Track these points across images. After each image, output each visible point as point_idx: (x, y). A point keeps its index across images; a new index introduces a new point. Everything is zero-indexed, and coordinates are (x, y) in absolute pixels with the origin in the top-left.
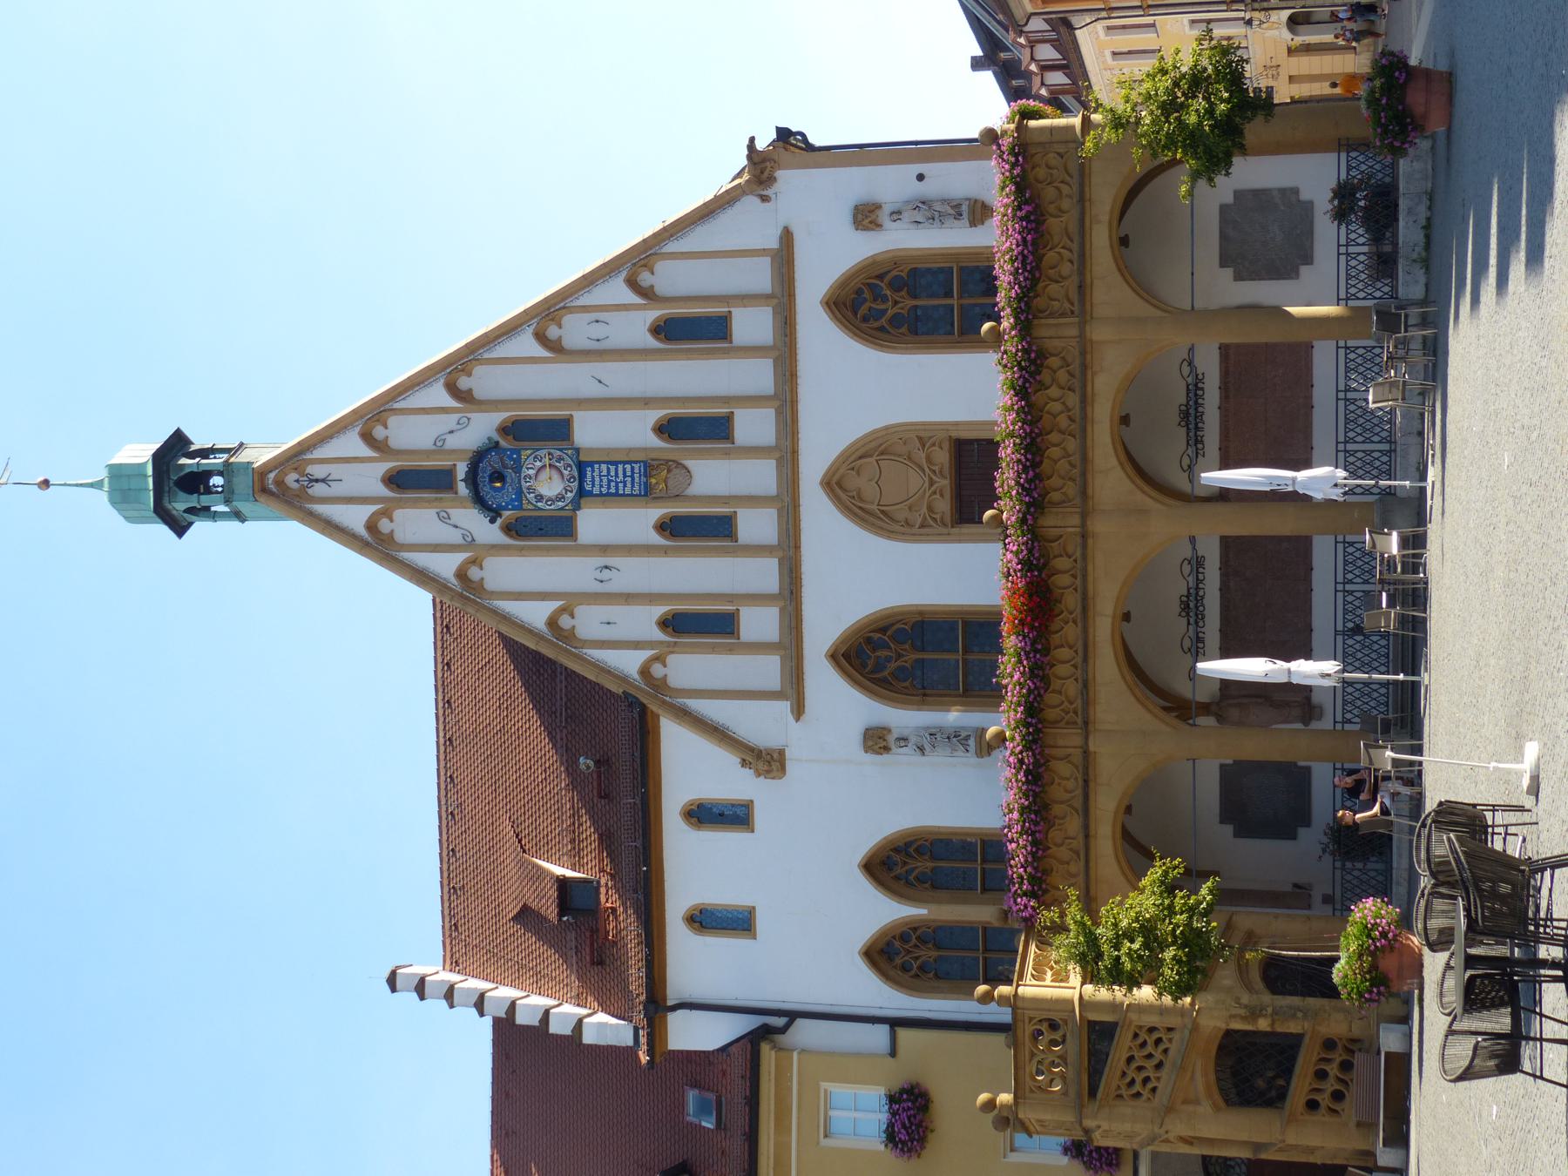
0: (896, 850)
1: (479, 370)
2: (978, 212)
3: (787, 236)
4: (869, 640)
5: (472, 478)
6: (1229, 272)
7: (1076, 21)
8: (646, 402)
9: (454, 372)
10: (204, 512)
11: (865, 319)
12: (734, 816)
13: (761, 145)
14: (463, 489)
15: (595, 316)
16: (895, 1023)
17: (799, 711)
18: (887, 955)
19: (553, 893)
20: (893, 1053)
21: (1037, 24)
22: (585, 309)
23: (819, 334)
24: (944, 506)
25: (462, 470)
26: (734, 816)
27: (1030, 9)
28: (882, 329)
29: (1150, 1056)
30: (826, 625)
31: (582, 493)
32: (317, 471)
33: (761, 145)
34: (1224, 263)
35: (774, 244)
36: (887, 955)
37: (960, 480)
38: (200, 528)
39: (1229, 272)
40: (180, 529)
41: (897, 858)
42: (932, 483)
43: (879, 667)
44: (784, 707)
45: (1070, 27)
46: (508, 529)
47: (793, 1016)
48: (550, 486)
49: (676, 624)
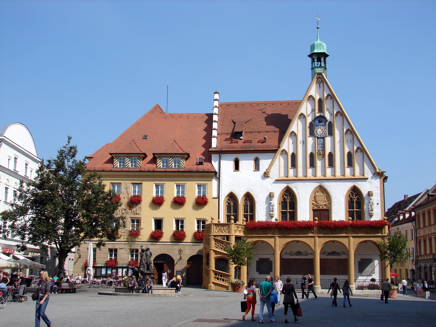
0: (251, 198)
1: (341, 117)
2: (371, 216)
3: (367, 179)
4: (291, 193)
5: (320, 116)
6: (360, 260)
7: (414, 223)
8: (335, 151)
9: (341, 113)
10: (313, 61)
11: (351, 193)
12: (257, 168)
13: (384, 173)
14: (318, 115)
15: (352, 140)
16: (219, 198)
17: (277, 180)
18: (232, 197)
19: (240, 130)
20: (213, 198)
21: (413, 214)
22: (353, 139)
23: (349, 185)
24: (316, 208)
25: (322, 114)
26: (257, 168)
27: (417, 212)
28: (350, 196)
29: (223, 247)
30: (294, 186)
31: (318, 138)
32: (321, 85)
33: (384, 173)
34: (362, 259)
35: (366, 176)
36: (232, 197)
37: (322, 213)
38: (310, 59)
39: (360, 260)
40: (310, 56)
41: (249, 198)
42: (321, 205)
43: (286, 195)
44: (278, 178)
45: (412, 221)
46: (311, 123)
47: (219, 179)
48: (319, 131)
49: (294, 156)
